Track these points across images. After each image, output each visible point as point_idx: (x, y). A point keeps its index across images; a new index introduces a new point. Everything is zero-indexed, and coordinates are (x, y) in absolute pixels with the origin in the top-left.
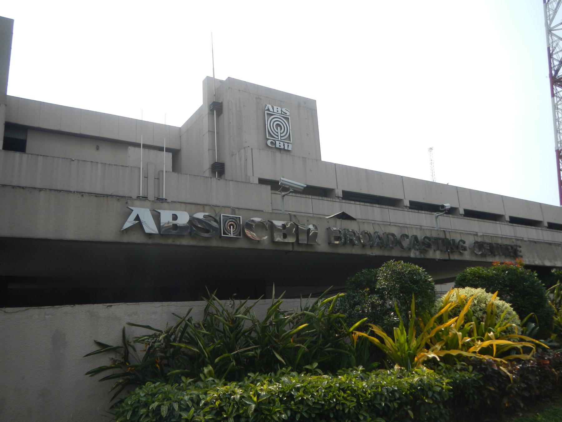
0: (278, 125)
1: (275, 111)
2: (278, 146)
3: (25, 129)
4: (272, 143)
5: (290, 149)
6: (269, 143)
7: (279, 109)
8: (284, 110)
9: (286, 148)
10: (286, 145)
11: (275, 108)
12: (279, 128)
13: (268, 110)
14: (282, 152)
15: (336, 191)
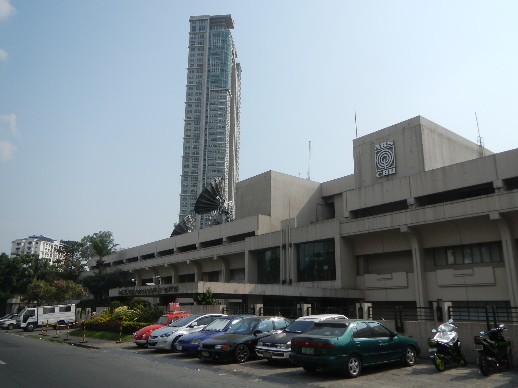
0: (385, 157)
1: (382, 147)
2: (384, 174)
3: (332, 197)
4: (380, 174)
5: (394, 172)
6: (377, 175)
7: (385, 143)
8: (389, 143)
9: (390, 173)
10: (390, 170)
11: (382, 145)
12: (385, 160)
13: (377, 149)
14: (390, 177)
15: (408, 201)
